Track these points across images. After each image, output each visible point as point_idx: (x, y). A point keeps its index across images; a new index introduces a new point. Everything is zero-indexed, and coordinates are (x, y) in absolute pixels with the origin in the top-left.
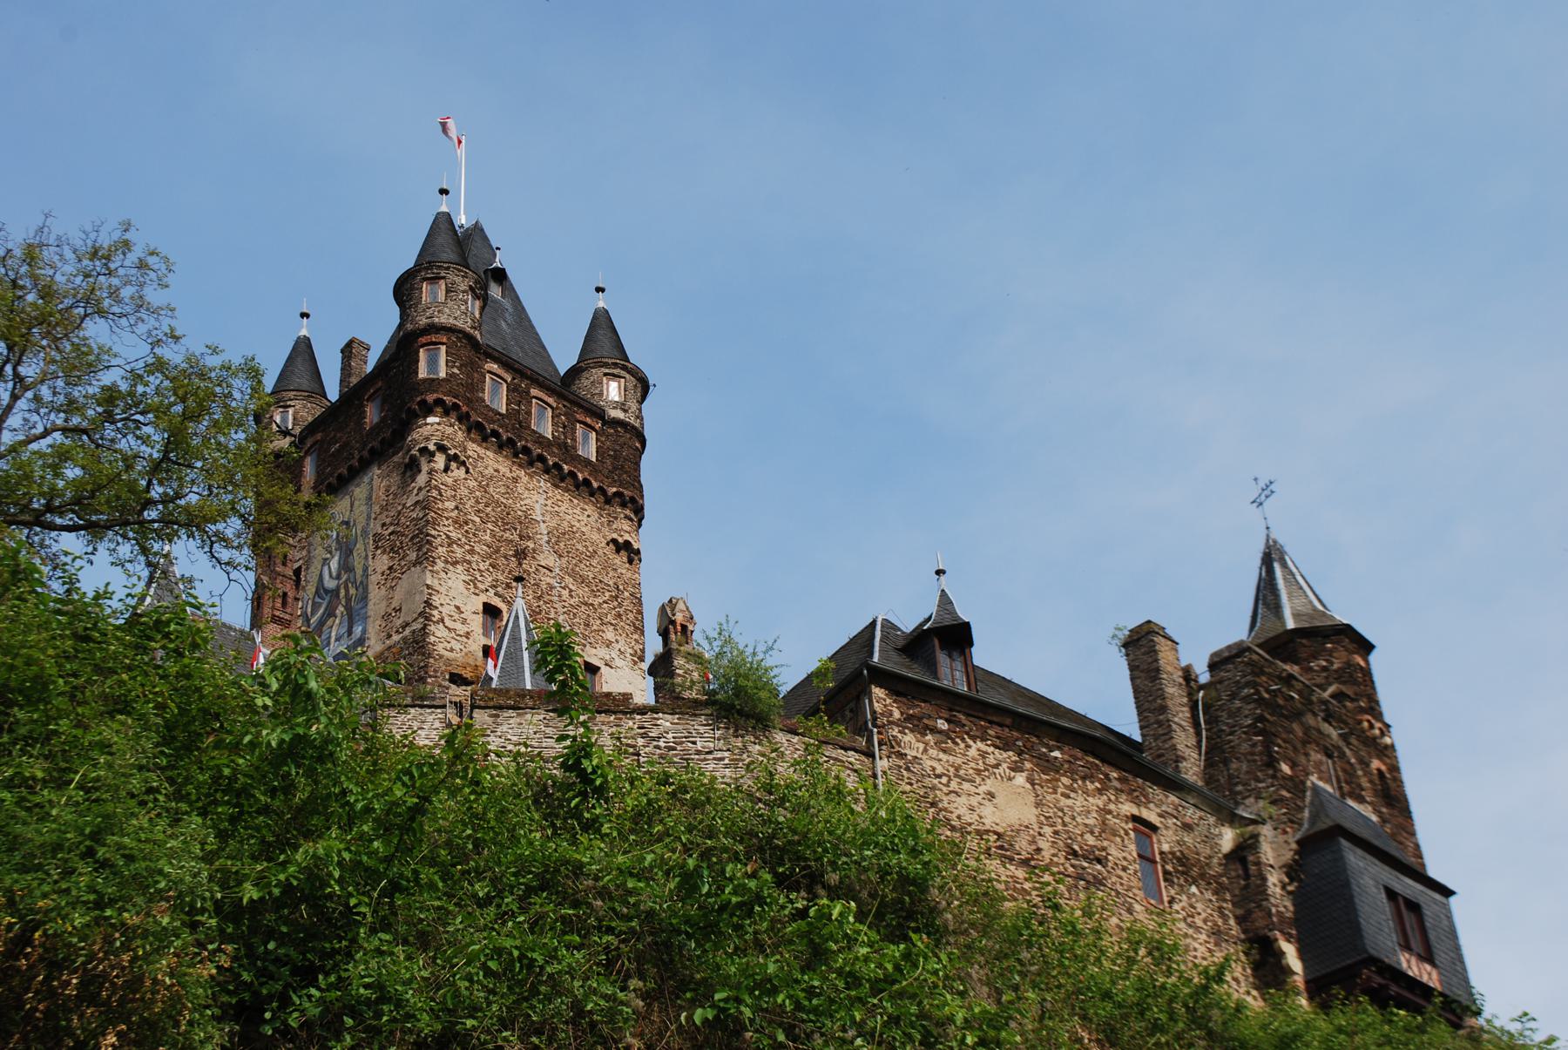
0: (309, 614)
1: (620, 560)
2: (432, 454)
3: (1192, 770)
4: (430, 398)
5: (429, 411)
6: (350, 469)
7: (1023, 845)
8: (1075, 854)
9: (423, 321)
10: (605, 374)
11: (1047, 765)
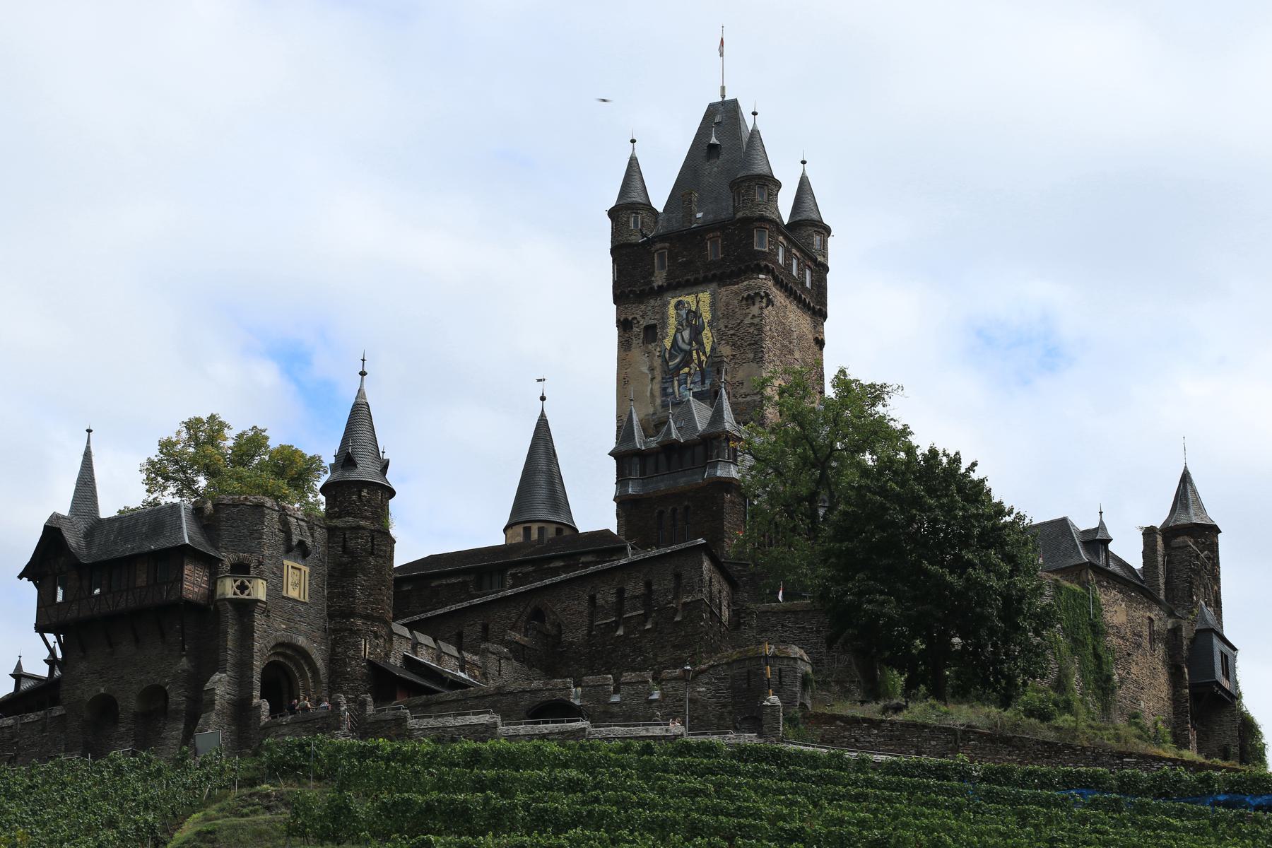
0: (667, 358)
1: (816, 349)
2: (762, 298)
3: (1162, 597)
4: (763, 263)
5: (761, 271)
6: (696, 279)
7: (1123, 631)
8: (1135, 634)
9: (757, 213)
10: (815, 231)
11: (1131, 599)
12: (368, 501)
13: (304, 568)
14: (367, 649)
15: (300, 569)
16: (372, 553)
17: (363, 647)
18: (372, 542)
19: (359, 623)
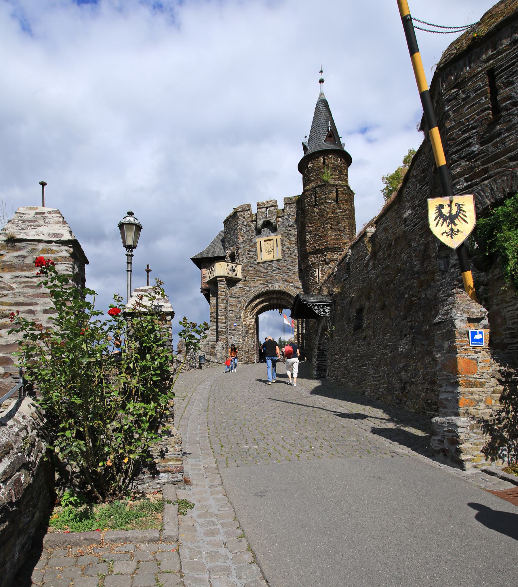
12: (312, 169)
13: (275, 238)
14: (320, 275)
15: (272, 240)
16: (316, 205)
17: (317, 274)
18: (316, 198)
19: (312, 258)
